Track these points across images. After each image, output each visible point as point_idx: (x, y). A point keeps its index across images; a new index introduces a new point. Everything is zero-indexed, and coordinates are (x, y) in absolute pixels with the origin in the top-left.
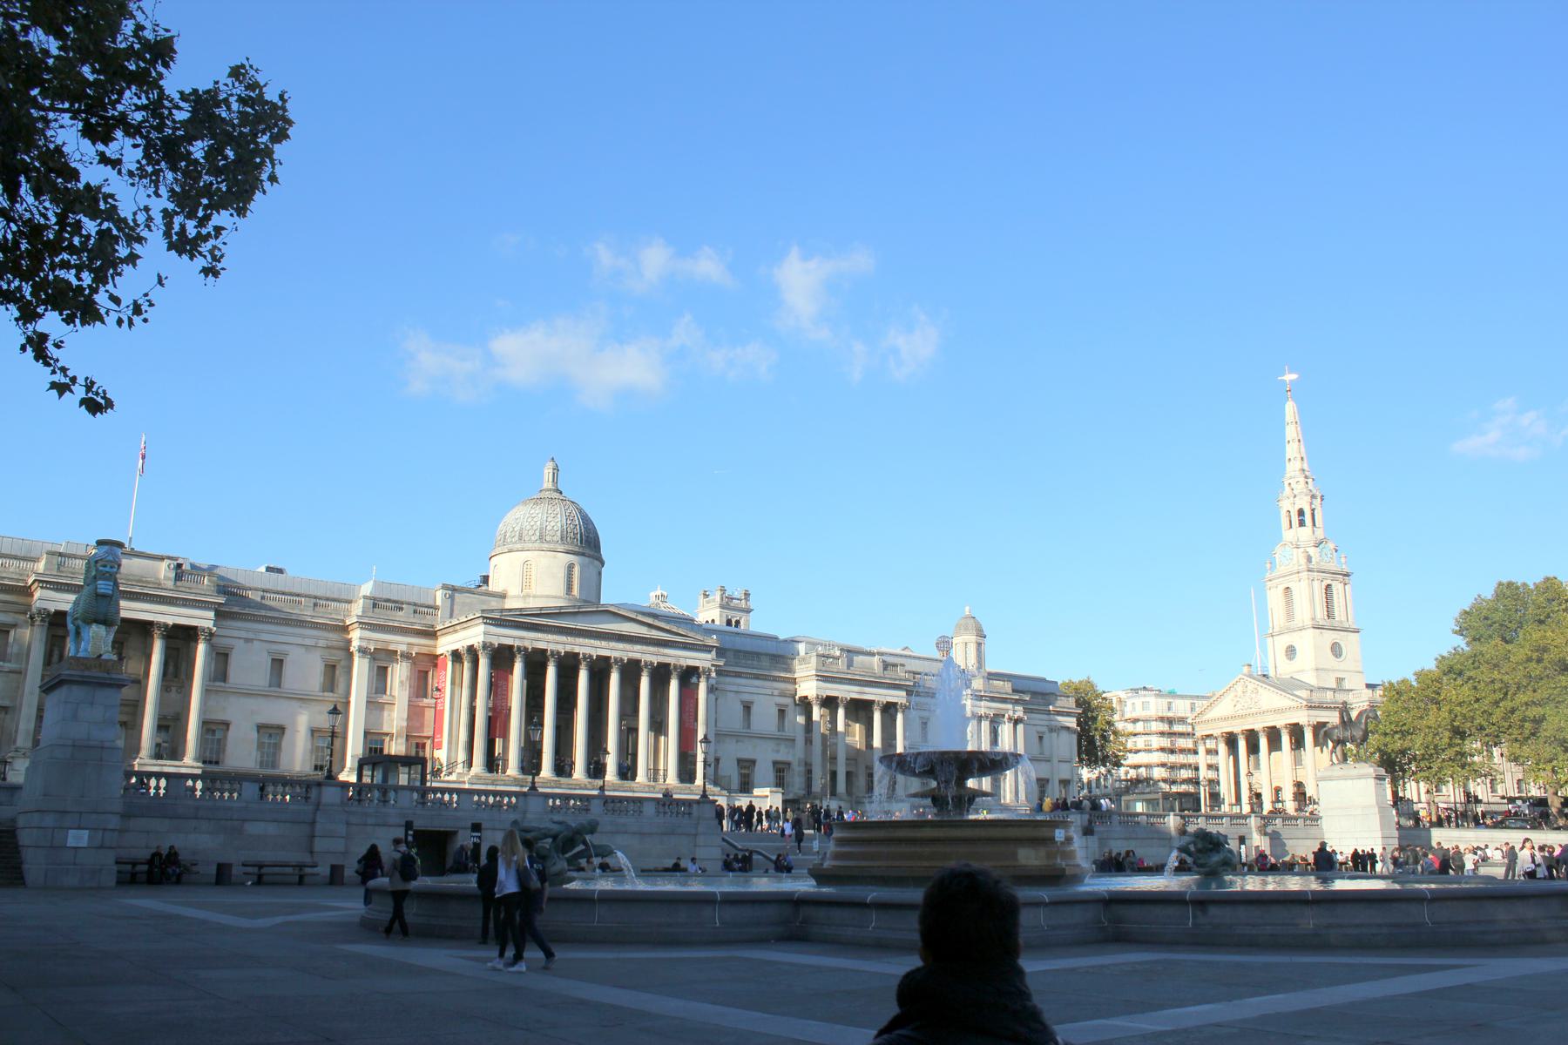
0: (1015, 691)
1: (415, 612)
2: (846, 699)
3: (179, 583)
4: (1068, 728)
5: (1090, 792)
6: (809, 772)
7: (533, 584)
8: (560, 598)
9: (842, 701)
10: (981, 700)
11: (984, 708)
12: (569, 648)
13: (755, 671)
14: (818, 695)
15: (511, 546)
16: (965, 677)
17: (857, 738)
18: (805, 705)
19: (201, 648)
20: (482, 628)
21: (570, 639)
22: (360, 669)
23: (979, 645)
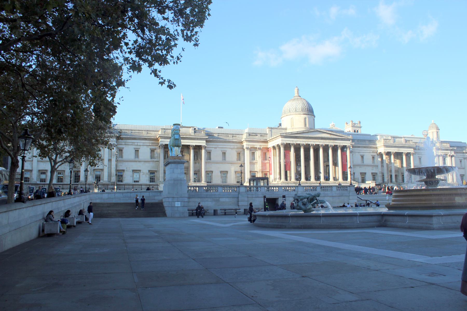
0: (451, 146)
1: (261, 136)
3: (195, 134)
6: (383, 175)
8: (303, 128)
9: (392, 153)
11: (440, 152)
12: (307, 143)
13: (364, 146)
14: (384, 152)
15: (287, 114)
16: (433, 143)
17: (398, 164)
18: (381, 155)
19: (203, 151)
21: (307, 140)
22: (247, 153)
23: (437, 132)
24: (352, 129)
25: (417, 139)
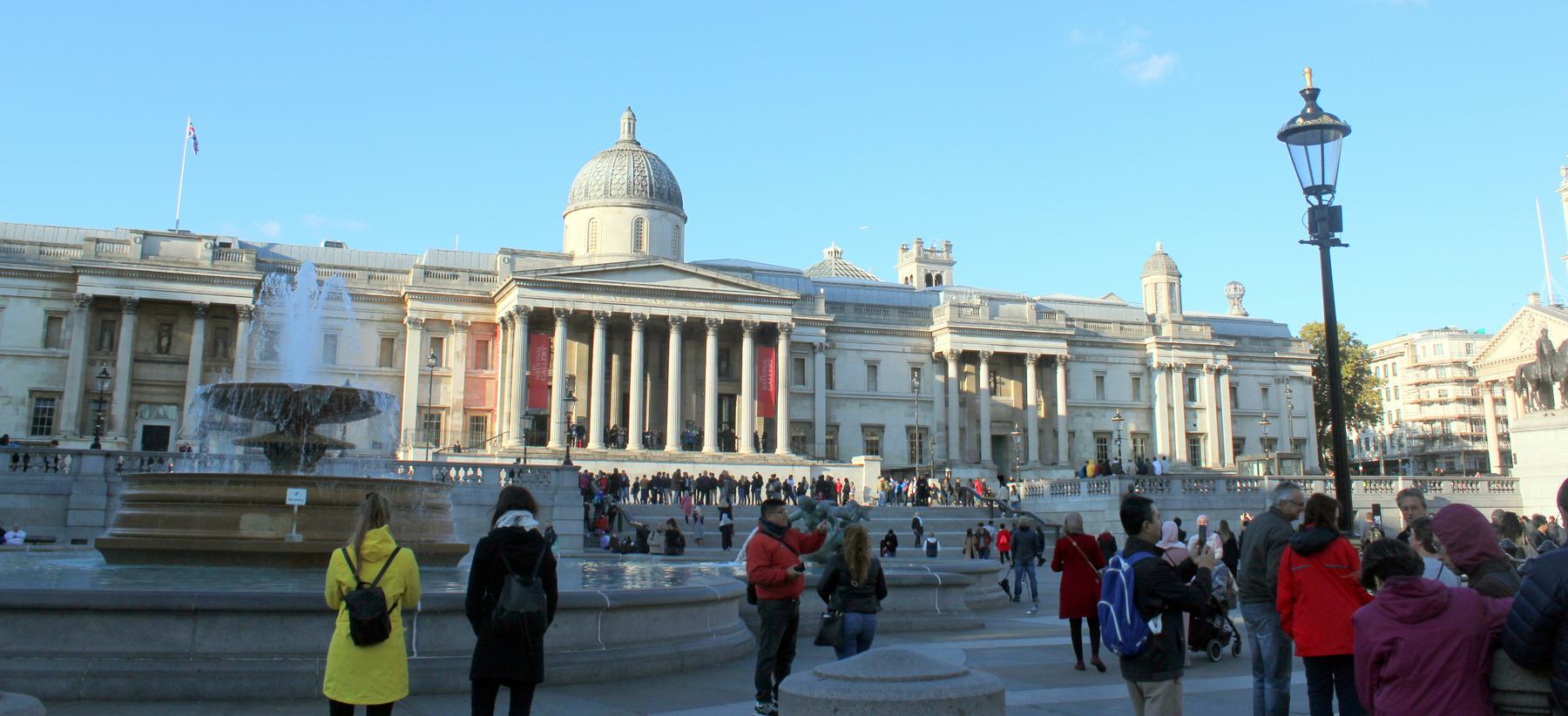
0: (1215, 336)
1: (471, 279)
2: (989, 353)
3: (216, 262)
4: (1301, 378)
5: (1385, 452)
7: (598, 243)
9: (983, 355)
10: (1171, 349)
11: (1174, 357)
12: (617, 309)
13: (880, 326)
15: (577, 204)
16: (1153, 325)
17: (1012, 398)
18: (940, 360)
20: (517, 291)
21: (618, 299)
22: (414, 341)
23: (1171, 285)
24: (918, 271)
25: (1091, 307)
